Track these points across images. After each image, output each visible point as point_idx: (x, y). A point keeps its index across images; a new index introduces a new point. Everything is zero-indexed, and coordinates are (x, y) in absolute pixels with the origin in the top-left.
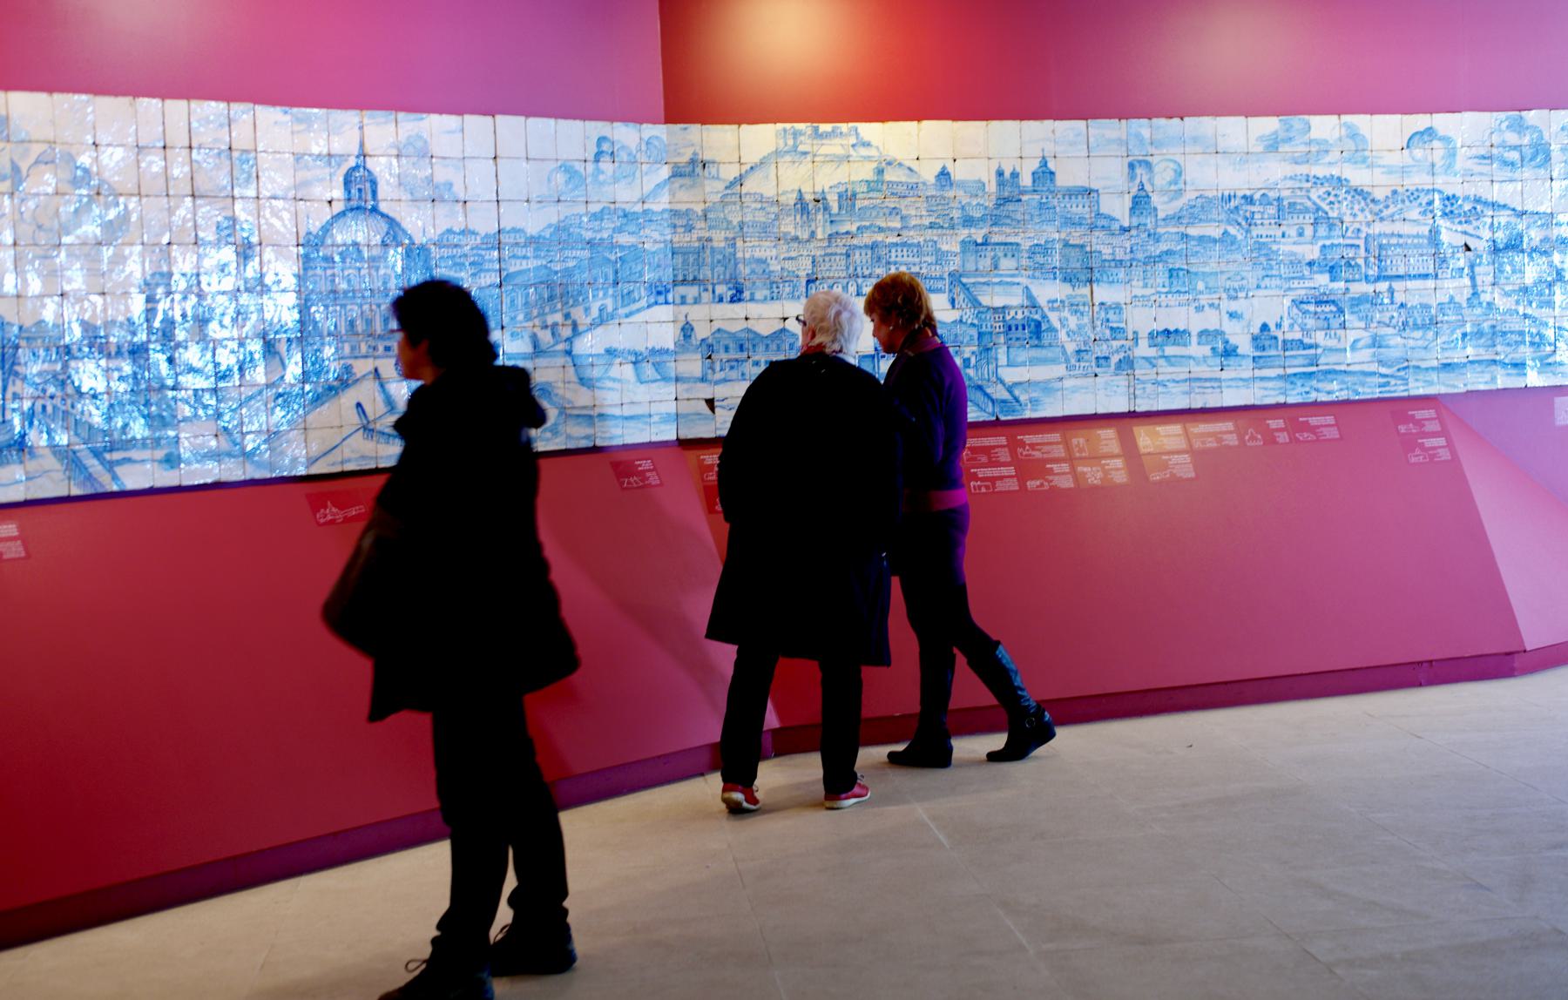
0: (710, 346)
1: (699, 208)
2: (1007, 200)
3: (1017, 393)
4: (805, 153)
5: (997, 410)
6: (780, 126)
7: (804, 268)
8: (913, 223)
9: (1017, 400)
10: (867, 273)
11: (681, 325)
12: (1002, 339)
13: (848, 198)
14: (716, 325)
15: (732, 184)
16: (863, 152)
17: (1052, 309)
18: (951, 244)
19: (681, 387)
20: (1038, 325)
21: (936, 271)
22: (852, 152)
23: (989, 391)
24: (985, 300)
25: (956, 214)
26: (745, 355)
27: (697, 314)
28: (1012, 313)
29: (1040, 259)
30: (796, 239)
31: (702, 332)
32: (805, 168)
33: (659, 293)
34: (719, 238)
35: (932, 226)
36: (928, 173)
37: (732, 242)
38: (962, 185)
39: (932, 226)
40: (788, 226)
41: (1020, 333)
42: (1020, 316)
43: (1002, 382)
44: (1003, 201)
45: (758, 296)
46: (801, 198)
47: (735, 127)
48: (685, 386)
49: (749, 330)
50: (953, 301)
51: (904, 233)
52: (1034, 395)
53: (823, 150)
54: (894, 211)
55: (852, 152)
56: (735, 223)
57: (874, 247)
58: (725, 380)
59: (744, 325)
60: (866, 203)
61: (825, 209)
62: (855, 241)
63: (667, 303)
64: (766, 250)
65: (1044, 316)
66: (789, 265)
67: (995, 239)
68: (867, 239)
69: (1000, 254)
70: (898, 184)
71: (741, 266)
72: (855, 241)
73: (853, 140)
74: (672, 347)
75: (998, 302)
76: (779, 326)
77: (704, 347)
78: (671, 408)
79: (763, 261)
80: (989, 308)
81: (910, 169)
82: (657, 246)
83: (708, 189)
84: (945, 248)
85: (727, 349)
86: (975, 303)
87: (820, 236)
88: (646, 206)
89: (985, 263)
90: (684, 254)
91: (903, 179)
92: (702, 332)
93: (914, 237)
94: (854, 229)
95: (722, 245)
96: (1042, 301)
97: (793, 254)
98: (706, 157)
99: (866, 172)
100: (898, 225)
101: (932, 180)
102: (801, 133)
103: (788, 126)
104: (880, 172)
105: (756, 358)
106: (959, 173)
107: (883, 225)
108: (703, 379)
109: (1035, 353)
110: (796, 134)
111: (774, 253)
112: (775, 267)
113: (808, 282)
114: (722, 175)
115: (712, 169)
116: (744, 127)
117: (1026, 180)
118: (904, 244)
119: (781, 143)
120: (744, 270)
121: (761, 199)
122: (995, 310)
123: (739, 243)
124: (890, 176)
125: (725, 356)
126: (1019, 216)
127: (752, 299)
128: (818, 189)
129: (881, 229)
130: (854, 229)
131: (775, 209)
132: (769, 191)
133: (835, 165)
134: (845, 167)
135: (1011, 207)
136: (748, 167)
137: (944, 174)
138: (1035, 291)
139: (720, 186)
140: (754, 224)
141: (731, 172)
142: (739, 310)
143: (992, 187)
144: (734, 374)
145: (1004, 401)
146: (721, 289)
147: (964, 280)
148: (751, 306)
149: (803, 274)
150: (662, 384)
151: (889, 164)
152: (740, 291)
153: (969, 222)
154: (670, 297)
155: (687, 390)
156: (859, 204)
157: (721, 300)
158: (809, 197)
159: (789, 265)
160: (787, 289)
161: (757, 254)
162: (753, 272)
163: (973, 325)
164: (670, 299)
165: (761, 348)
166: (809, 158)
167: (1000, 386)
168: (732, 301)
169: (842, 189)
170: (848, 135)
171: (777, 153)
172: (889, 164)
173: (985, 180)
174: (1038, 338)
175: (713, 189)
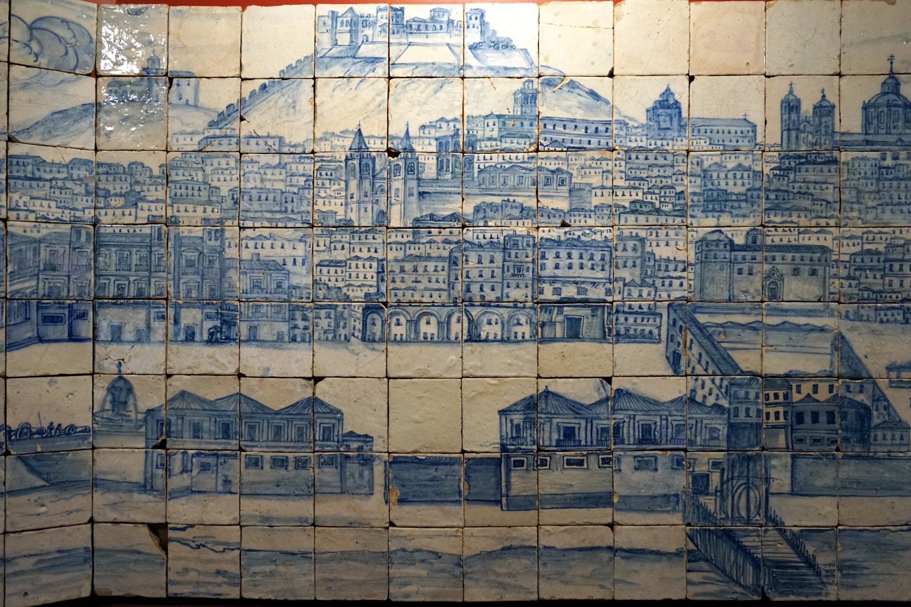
0: (165, 426)
1: (154, 162)
2: (805, 160)
3: (810, 549)
4: (374, 60)
5: (765, 581)
6: (324, 9)
7: (362, 281)
8: (596, 201)
9: (810, 563)
10: (491, 296)
11: (102, 383)
12: (781, 441)
13: (458, 150)
14: (178, 384)
15: (222, 118)
16: (495, 59)
17: (898, 384)
18: (675, 247)
19: (100, 498)
20: (864, 413)
21: (641, 297)
22: (470, 59)
23: (748, 542)
24: (747, 360)
25: (690, 186)
26: (234, 444)
27: (142, 360)
28: (807, 388)
29: (874, 281)
30: (346, 225)
31: (149, 397)
32: (372, 90)
33: (54, 320)
34: (192, 219)
35: (636, 208)
36: (633, 102)
37: (217, 228)
38: (703, 127)
39: (636, 208)
40: (333, 202)
41: (822, 430)
42: (823, 394)
43: (778, 524)
44: (792, 162)
45: (265, 332)
46: (360, 147)
47: (235, 10)
48: (111, 497)
49: (240, 397)
50: (674, 360)
51: (576, 220)
52: (849, 555)
53: (412, 55)
54: (558, 177)
55: (470, 59)
56: (224, 192)
57: (508, 245)
58: (190, 491)
59: (229, 387)
60: (496, 158)
61: (410, 169)
62: (469, 235)
63: (73, 338)
64: (287, 247)
65: (879, 398)
66: (328, 276)
67: (775, 237)
68: (494, 230)
69: (784, 269)
70: (564, 122)
71: (233, 275)
72: (469, 235)
73: (473, 36)
74: (84, 420)
75: (777, 364)
76: (302, 392)
77: (152, 424)
78: (80, 538)
79: (280, 267)
80: (754, 375)
81: (593, 94)
82: (45, 230)
83: (175, 126)
84: (663, 252)
85: (197, 432)
86: (724, 365)
87: (395, 222)
88: (15, 149)
89: (751, 286)
90: (121, 246)
91: (580, 115)
92: (149, 397)
93: (598, 229)
94: (468, 209)
95: (198, 232)
96: (875, 366)
97: (339, 255)
98: (176, 66)
99: (498, 98)
100: (563, 205)
101: (642, 118)
102: (366, 22)
103: (341, 8)
104: (529, 98)
105: (255, 452)
106: (700, 103)
107: (532, 203)
108: (146, 487)
109: (850, 470)
110: (356, 24)
111: (301, 250)
112: (301, 278)
113: (367, 310)
114: (203, 100)
115: (187, 89)
116: (253, 9)
117: (850, 121)
118: (572, 243)
119: (325, 40)
120: (239, 282)
121: (279, 147)
122: (769, 380)
123: (231, 232)
124: (552, 106)
125: (192, 445)
126: (830, 194)
127: (253, 339)
128: (397, 129)
129: (524, 212)
130: (468, 209)
131: (308, 167)
132: (297, 132)
133: (434, 84)
134: (456, 86)
135: (811, 174)
136: (256, 85)
137: (666, 105)
138: (861, 343)
139: (200, 121)
140: (262, 195)
141: (220, 95)
142: (223, 358)
143: (773, 135)
144: (208, 481)
145: (780, 565)
146: (190, 317)
147: (702, 319)
148: (248, 351)
149: (359, 294)
150: (47, 496)
151: (549, 83)
152: (228, 322)
153: (717, 201)
154: (85, 328)
155: (113, 505)
156: (479, 161)
157: (190, 337)
158: (376, 145)
159: (328, 276)
160: (324, 323)
161: (266, 253)
162: (256, 286)
163: (717, 407)
164: (85, 328)
165: (265, 433)
166: (381, 69)
167: (773, 534)
168: (212, 340)
169: (446, 131)
170: (464, 27)
171: (316, 59)
172: (549, 83)
173: (757, 118)
174: (864, 440)
175: (186, 128)
